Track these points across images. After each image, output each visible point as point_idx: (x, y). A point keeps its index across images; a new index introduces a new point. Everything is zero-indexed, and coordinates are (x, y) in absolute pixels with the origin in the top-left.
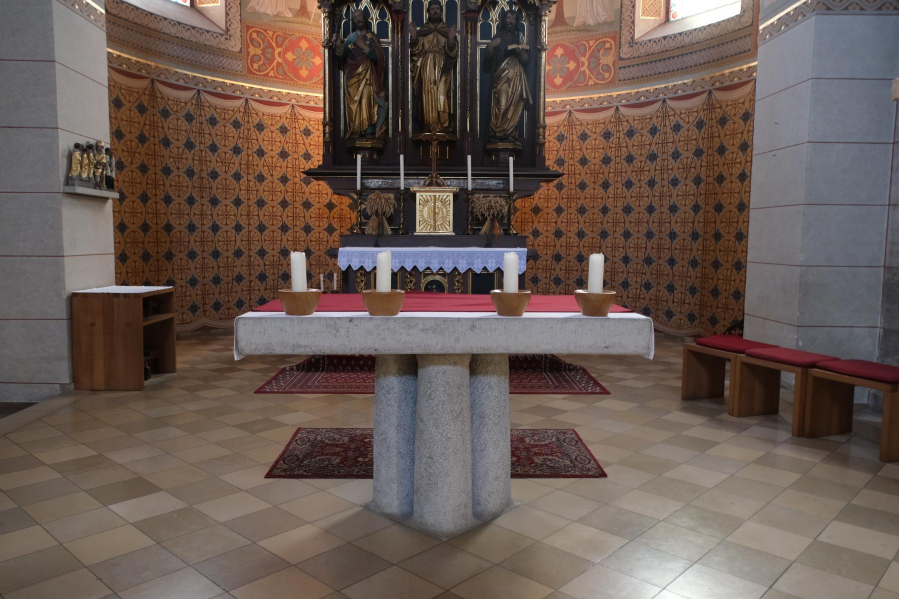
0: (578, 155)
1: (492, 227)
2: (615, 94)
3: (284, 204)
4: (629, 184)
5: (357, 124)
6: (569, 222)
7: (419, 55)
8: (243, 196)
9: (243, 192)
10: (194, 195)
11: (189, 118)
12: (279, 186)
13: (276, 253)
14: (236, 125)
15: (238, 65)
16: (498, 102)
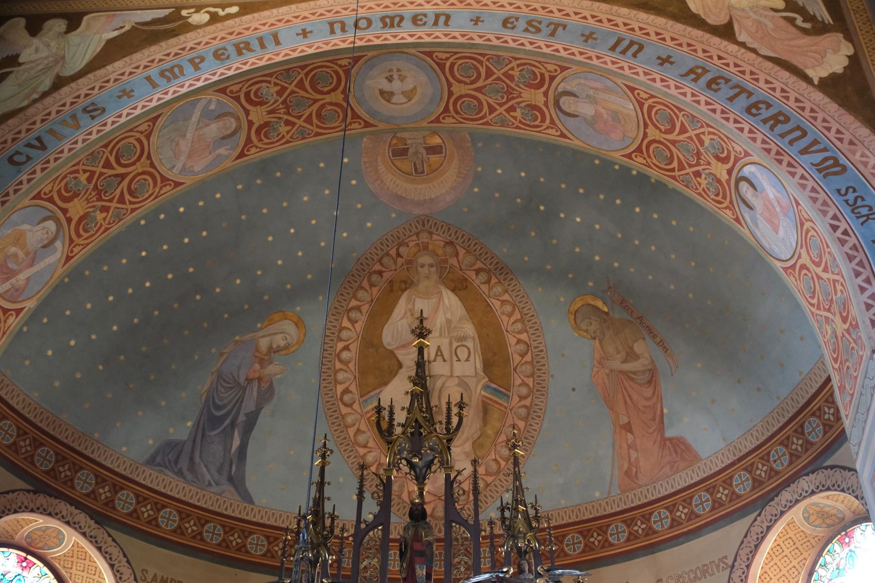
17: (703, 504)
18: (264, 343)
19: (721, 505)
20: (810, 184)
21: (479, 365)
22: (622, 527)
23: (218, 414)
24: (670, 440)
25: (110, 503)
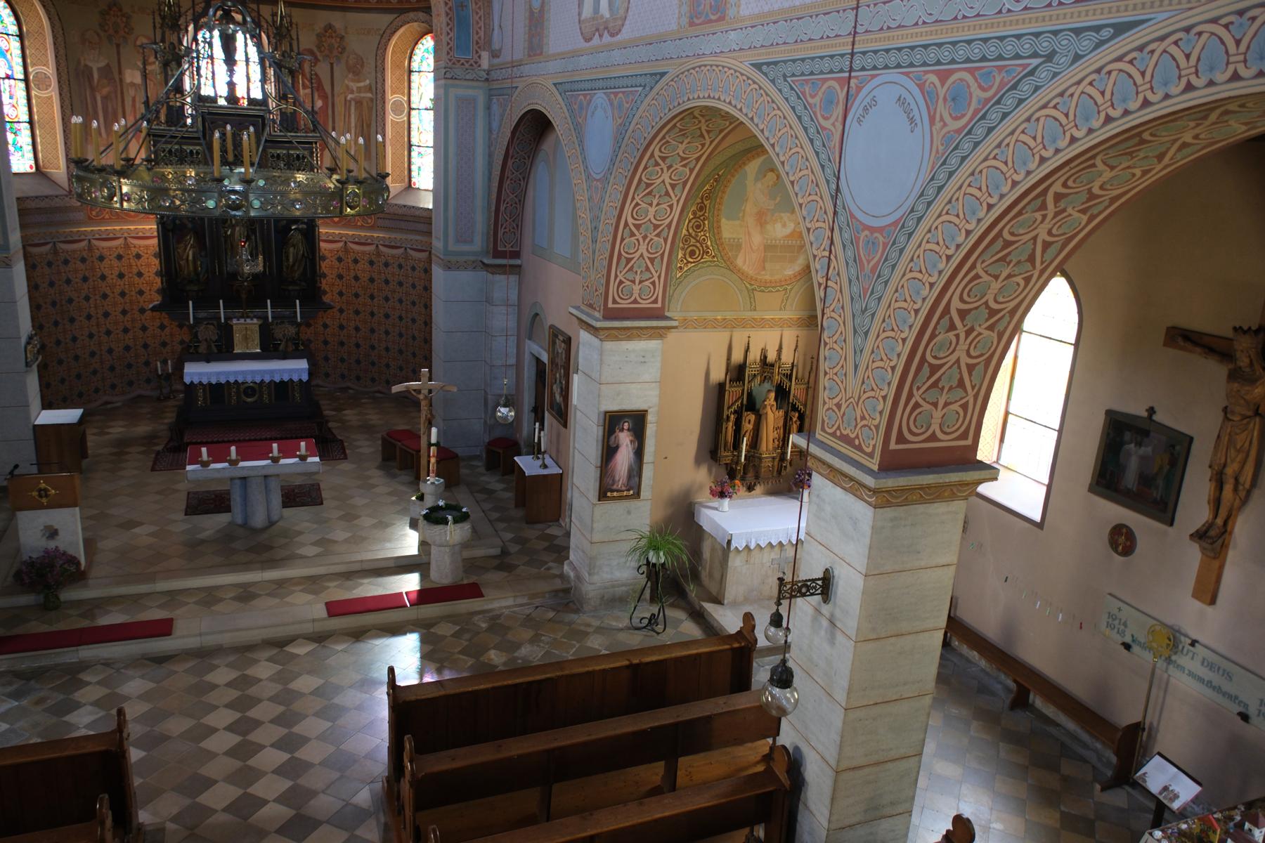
1: (287, 346)
2: (375, 235)
3: (124, 312)
4: (387, 299)
5: (186, 272)
8: (93, 312)
9: (92, 309)
10: (58, 319)
11: (50, 264)
12: (120, 299)
14: (83, 260)
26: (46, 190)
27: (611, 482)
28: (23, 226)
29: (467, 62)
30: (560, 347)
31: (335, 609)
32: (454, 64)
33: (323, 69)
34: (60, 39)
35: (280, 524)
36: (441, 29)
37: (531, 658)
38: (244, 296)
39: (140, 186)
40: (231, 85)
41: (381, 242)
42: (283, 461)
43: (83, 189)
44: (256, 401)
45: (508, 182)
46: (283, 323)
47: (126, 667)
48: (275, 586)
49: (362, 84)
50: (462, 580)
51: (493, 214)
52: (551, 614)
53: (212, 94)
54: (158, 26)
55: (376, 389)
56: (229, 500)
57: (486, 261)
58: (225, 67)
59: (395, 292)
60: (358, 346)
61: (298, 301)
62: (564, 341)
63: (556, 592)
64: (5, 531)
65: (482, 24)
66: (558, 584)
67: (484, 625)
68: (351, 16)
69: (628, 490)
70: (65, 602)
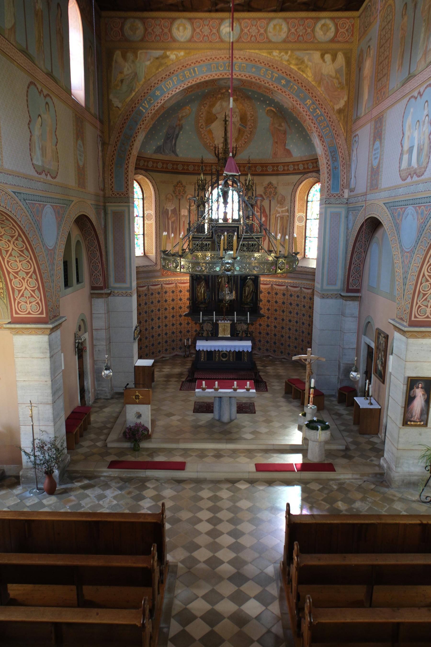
0: (274, 300)
1: (242, 335)
3: (173, 317)
4: (290, 312)
5: (200, 299)
6: (271, 322)
7: (220, 278)
8: (161, 316)
11: (146, 295)
13: (170, 333)
14: (159, 293)
15: (159, 274)
16: (245, 293)
17: (291, 168)
18: (180, 116)
19: (295, 170)
20: (326, 148)
21: (239, 119)
22: (271, 167)
23: (169, 136)
24: (287, 149)
25: (147, 166)
26: (147, 263)
27: (410, 416)
28: (138, 279)
29: (337, 195)
30: (382, 340)
31: (260, 468)
32: (330, 196)
33: (266, 203)
34: (158, 199)
35: (235, 421)
36: (325, 180)
37: (361, 510)
38: (224, 310)
39: (189, 262)
40: (225, 213)
41: (289, 285)
42: (239, 391)
43: (165, 264)
44: (227, 360)
45: (356, 254)
46: (241, 323)
47: (165, 483)
48: (232, 452)
49: (284, 209)
50: (324, 460)
51: (347, 270)
52: (373, 487)
53: (216, 218)
54: (196, 189)
55: (282, 357)
56: (213, 407)
57: (342, 294)
58: (223, 205)
59: (294, 309)
60: (275, 335)
61: (248, 313)
62: (384, 337)
63: (376, 474)
64: (120, 412)
65: (345, 176)
66: (377, 470)
67: (335, 487)
68: (281, 177)
69: (421, 422)
70: (142, 448)
